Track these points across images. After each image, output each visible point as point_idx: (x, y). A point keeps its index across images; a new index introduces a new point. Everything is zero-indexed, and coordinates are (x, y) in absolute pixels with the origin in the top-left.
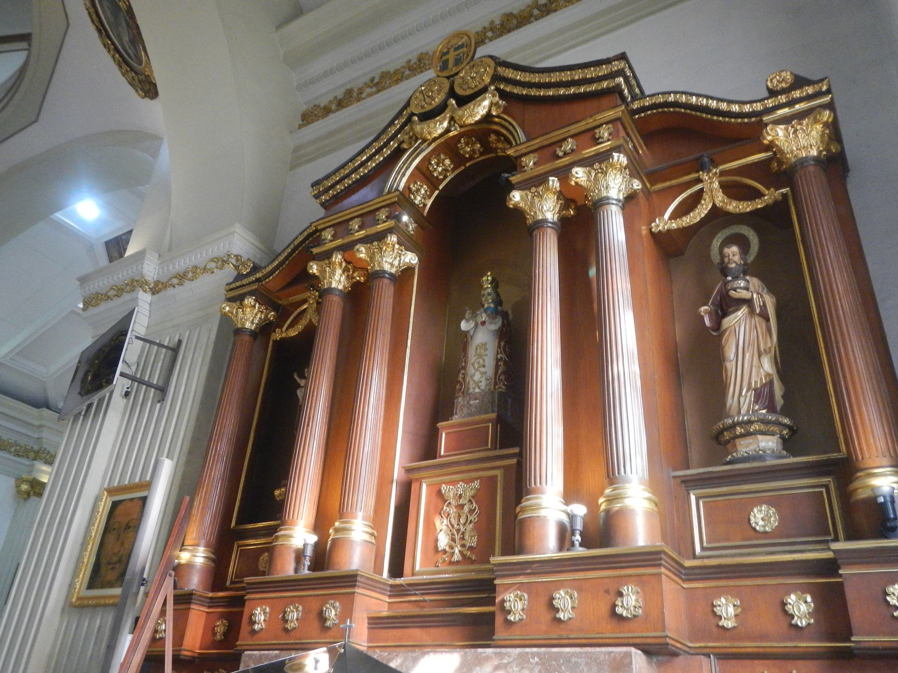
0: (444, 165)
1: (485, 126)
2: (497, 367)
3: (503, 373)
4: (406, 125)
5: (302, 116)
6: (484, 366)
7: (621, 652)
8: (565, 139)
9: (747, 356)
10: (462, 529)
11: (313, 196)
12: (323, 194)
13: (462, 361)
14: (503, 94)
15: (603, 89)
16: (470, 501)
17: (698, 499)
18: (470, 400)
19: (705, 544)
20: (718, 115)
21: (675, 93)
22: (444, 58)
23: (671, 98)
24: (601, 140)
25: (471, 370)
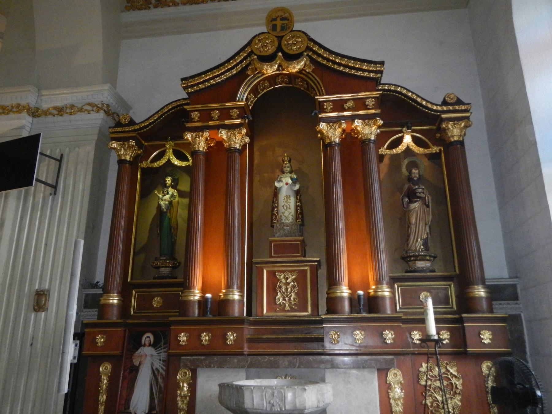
1: (298, 74)
2: (296, 210)
6: (290, 209)
9: (421, 224)
10: (289, 296)
14: (312, 61)
17: (398, 287)
18: (284, 226)
19: (401, 306)
21: (402, 87)
22: (274, 23)
23: (399, 89)
25: (281, 210)
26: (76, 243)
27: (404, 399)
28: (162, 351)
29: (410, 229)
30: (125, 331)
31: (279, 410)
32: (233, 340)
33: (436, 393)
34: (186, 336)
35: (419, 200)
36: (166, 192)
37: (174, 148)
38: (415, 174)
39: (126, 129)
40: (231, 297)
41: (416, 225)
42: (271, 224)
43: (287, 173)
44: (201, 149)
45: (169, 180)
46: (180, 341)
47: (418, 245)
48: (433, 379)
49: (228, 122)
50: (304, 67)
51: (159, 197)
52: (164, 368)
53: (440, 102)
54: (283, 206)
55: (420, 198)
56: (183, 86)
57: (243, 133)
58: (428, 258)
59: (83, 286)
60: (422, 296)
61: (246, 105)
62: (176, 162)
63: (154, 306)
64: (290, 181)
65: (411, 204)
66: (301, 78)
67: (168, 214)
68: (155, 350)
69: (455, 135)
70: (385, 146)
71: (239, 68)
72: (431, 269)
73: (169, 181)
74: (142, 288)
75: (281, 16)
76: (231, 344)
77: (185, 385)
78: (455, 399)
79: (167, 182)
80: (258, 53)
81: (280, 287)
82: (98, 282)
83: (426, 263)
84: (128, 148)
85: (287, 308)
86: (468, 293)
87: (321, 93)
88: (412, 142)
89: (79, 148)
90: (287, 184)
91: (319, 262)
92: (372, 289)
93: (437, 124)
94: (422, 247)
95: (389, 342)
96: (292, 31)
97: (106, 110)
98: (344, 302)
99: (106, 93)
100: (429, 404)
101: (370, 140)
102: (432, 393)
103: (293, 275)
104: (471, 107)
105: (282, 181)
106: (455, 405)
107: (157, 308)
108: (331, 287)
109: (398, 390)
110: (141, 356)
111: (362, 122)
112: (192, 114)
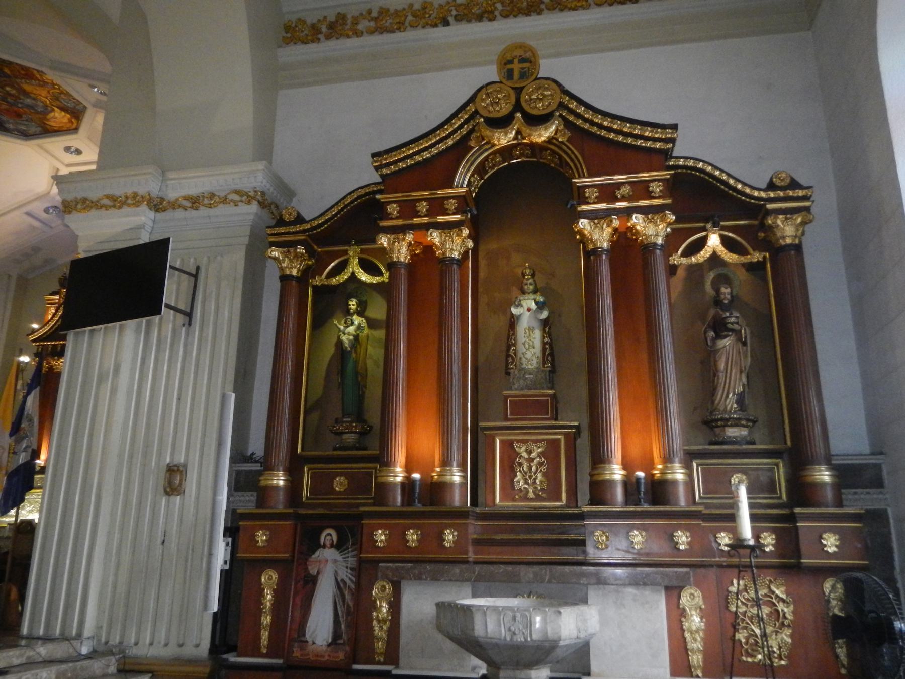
1: (545, 144)
2: (544, 349)
3: (548, 354)
5: (284, 28)
6: (534, 347)
7: (682, 572)
9: (734, 371)
10: (534, 477)
13: (512, 339)
14: (568, 124)
16: (539, 456)
17: (698, 466)
18: (525, 373)
19: (702, 495)
21: (705, 162)
22: (509, 67)
23: (700, 165)
25: (521, 349)
26: (224, 398)
27: (705, 631)
28: (350, 554)
29: (716, 378)
30: (296, 525)
31: (523, 640)
32: (453, 541)
33: (754, 625)
34: (385, 534)
35: (731, 335)
36: (350, 323)
37: (361, 255)
38: (725, 294)
39: (292, 229)
40: (448, 478)
41: (726, 372)
42: (506, 370)
43: (529, 293)
44: (402, 260)
45: (353, 304)
46: (376, 541)
47: (729, 404)
48: (749, 604)
49: (441, 219)
50: (556, 133)
51: (340, 329)
52: (354, 579)
53: (764, 185)
54: (524, 344)
55: (732, 330)
56: (374, 165)
57: (464, 235)
58: (744, 423)
59: (234, 460)
60: (734, 480)
61: (469, 192)
62: (364, 277)
63: (335, 490)
64: (534, 306)
66: (551, 150)
67: (354, 355)
68: (340, 553)
69: (787, 236)
70: (679, 252)
71: (457, 136)
72: (748, 439)
73: (353, 305)
74: (319, 463)
75: (520, 56)
76: (450, 547)
77: (384, 604)
78: (781, 633)
80: (486, 114)
81: (520, 464)
82: (253, 454)
83: (741, 430)
84: (294, 257)
85: (531, 495)
86: (805, 476)
87: (581, 174)
89: (222, 256)
90: (529, 310)
91: (578, 428)
92: (658, 469)
93: (760, 217)
94: (735, 406)
95: (682, 547)
96: (537, 79)
97: (261, 200)
98: (615, 487)
99: (260, 176)
100: (743, 641)
101: (655, 244)
102: (747, 623)
103: (539, 447)
104: (813, 192)
105: (522, 306)
106: (782, 643)
107: (340, 493)
108: (597, 466)
109: (697, 619)
110: (320, 561)
111: (643, 218)
112: (388, 207)
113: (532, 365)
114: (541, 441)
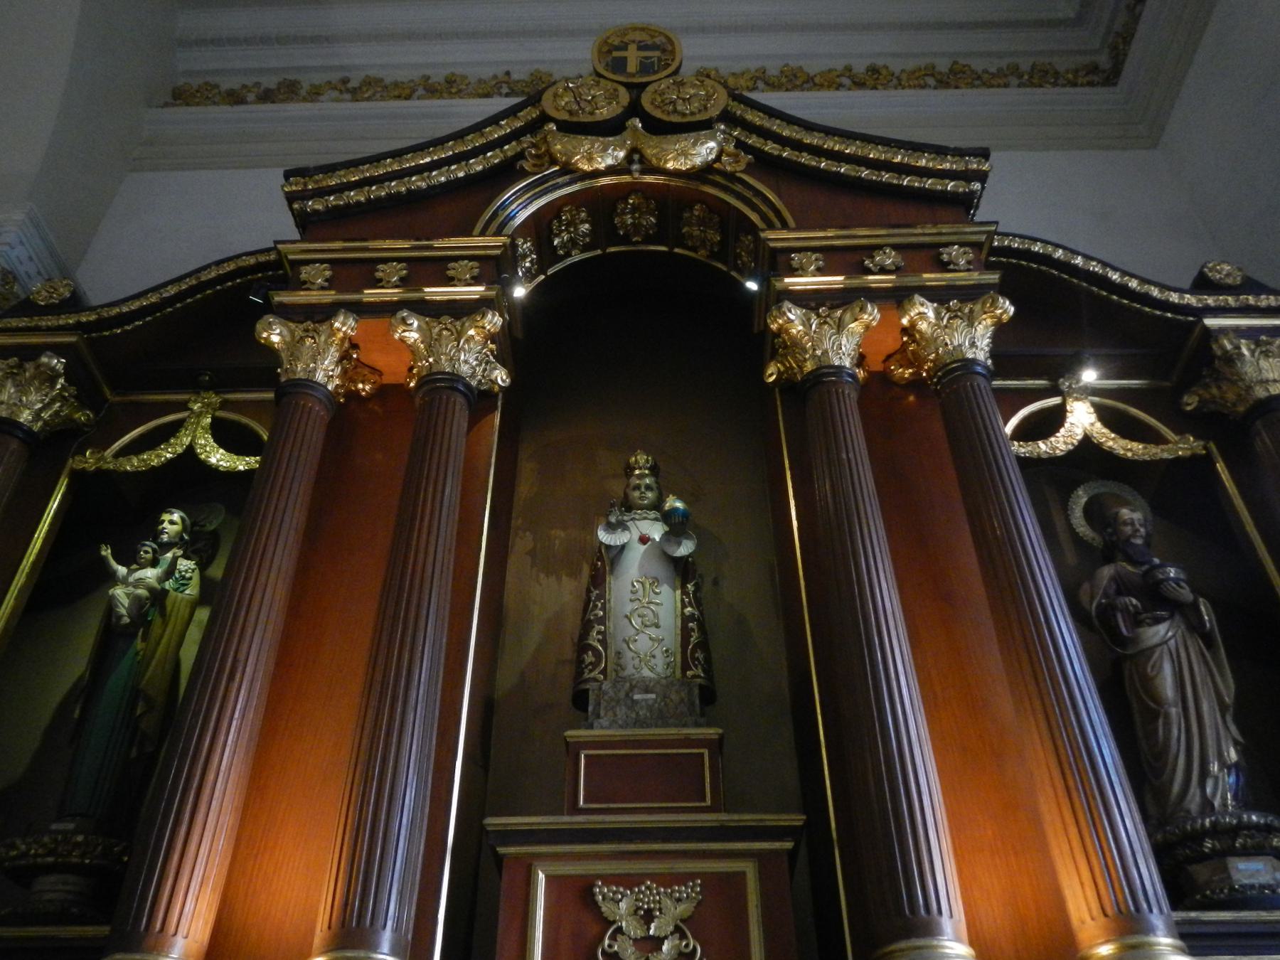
0: (576, 229)
2: (685, 633)
4: (509, 143)
6: (657, 626)
8: (880, 247)
11: (286, 193)
12: (311, 198)
15: (944, 192)
16: (677, 929)
18: (632, 688)
20: (1121, 296)
22: (616, 54)
23: (1037, 248)
24: (951, 267)
29: (1161, 722)
36: (149, 556)
45: (172, 522)
47: (1214, 794)
49: (436, 293)
50: (718, 159)
53: (1187, 283)
62: (218, 457)
64: (656, 531)
65: (1141, 630)
73: (172, 522)
75: (640, 42)
79: (166, 525)
88: (1099, 425)
90: (644, 540)
103: (679, 900)
113: (652, 669)
114: (682, 879)
